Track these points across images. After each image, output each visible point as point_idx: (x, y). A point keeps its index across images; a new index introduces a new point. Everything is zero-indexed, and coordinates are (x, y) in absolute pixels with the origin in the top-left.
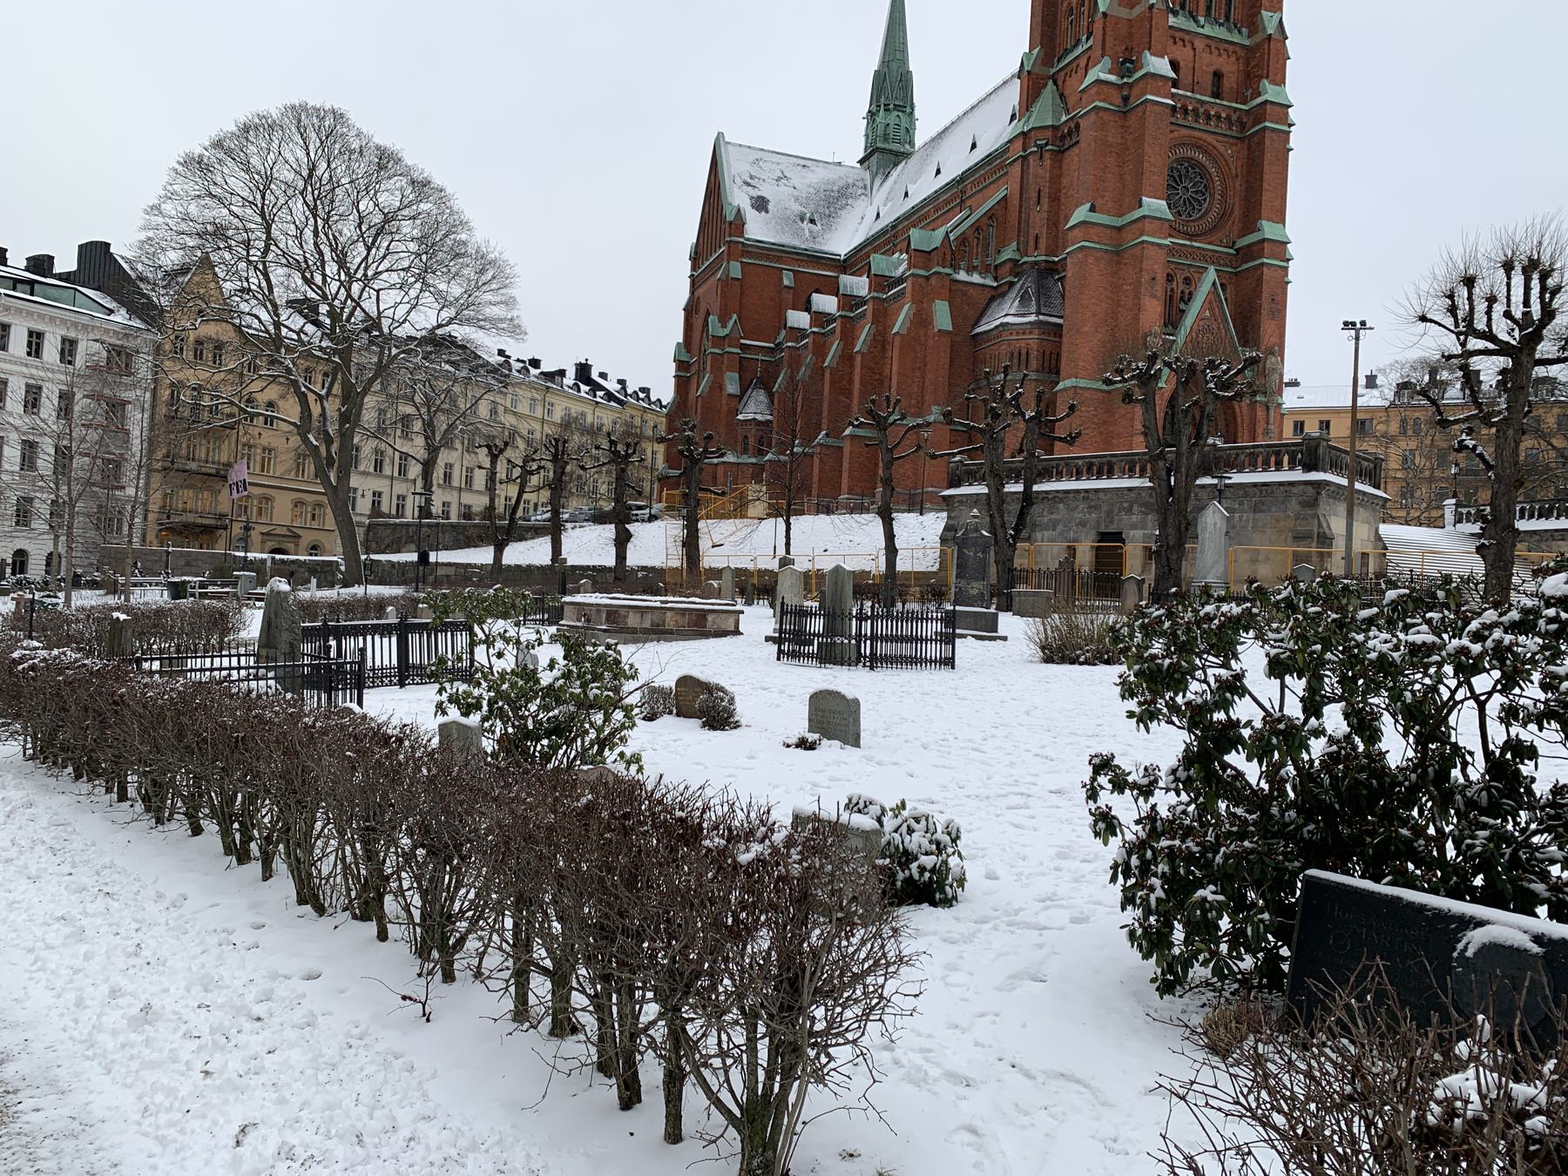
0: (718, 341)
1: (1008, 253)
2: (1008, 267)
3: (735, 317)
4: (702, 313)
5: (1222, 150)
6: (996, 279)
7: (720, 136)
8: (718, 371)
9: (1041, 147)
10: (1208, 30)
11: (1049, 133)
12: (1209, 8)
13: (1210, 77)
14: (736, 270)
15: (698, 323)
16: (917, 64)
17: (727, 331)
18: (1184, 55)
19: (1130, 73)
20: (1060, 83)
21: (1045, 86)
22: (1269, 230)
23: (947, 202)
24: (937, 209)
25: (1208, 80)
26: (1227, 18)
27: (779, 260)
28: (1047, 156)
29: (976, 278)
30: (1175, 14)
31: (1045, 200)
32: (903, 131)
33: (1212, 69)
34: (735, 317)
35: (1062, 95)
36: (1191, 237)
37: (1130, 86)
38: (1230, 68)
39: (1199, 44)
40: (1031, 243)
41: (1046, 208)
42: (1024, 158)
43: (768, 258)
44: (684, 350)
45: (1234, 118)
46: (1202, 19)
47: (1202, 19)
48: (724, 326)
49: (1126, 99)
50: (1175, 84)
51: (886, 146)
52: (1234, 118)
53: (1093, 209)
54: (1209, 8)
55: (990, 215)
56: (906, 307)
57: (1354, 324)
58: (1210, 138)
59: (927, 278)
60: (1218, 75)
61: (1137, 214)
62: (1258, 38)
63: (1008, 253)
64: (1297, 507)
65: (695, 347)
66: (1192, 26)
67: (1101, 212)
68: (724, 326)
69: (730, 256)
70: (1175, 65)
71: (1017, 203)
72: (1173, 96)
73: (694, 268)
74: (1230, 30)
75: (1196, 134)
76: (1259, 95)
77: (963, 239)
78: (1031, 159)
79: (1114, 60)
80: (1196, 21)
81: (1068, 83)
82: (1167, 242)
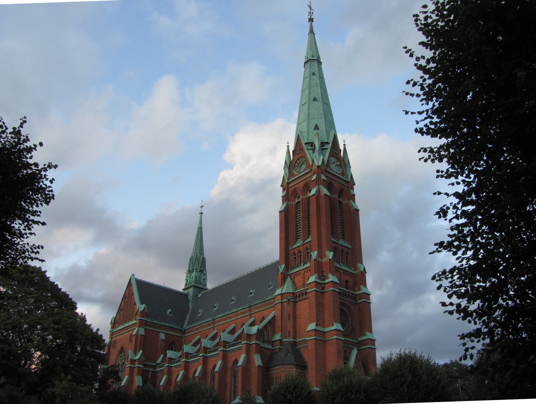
0: (133, 361)
1: (278, 337)
2: (279, 342)
6: (273, 346)
7: (133, 275)
8: (131, 374)
9: (289, 299)
10: (343, 268)
11: (292, 295)
14: (142, 332)
19: (324, 280)
20: (292, 278)
21: (287, 278)
24: (236, 315)
27: (159, 328)
31: (291, 318)
32: (202, 279)
34: (141, 351)
35: (294, 282)
37: (325, 284)
39: (341, 272)
40: (287, 334)
41: (292, 321)
42: (282, 303)
43: (154, 327)
45: (353, 296)
49: (323, 288)
52: (353, 296)
53: (317, 325)
55: (270, 322)
58: (347, 303)
60: (347, 282)
63: (278, 337)
66: (339, 266)
71: (280, 318)
72: (339, 289)
78: (285, 304)
80: (340, 265)
81: (296, 278)
82: (343, 338)
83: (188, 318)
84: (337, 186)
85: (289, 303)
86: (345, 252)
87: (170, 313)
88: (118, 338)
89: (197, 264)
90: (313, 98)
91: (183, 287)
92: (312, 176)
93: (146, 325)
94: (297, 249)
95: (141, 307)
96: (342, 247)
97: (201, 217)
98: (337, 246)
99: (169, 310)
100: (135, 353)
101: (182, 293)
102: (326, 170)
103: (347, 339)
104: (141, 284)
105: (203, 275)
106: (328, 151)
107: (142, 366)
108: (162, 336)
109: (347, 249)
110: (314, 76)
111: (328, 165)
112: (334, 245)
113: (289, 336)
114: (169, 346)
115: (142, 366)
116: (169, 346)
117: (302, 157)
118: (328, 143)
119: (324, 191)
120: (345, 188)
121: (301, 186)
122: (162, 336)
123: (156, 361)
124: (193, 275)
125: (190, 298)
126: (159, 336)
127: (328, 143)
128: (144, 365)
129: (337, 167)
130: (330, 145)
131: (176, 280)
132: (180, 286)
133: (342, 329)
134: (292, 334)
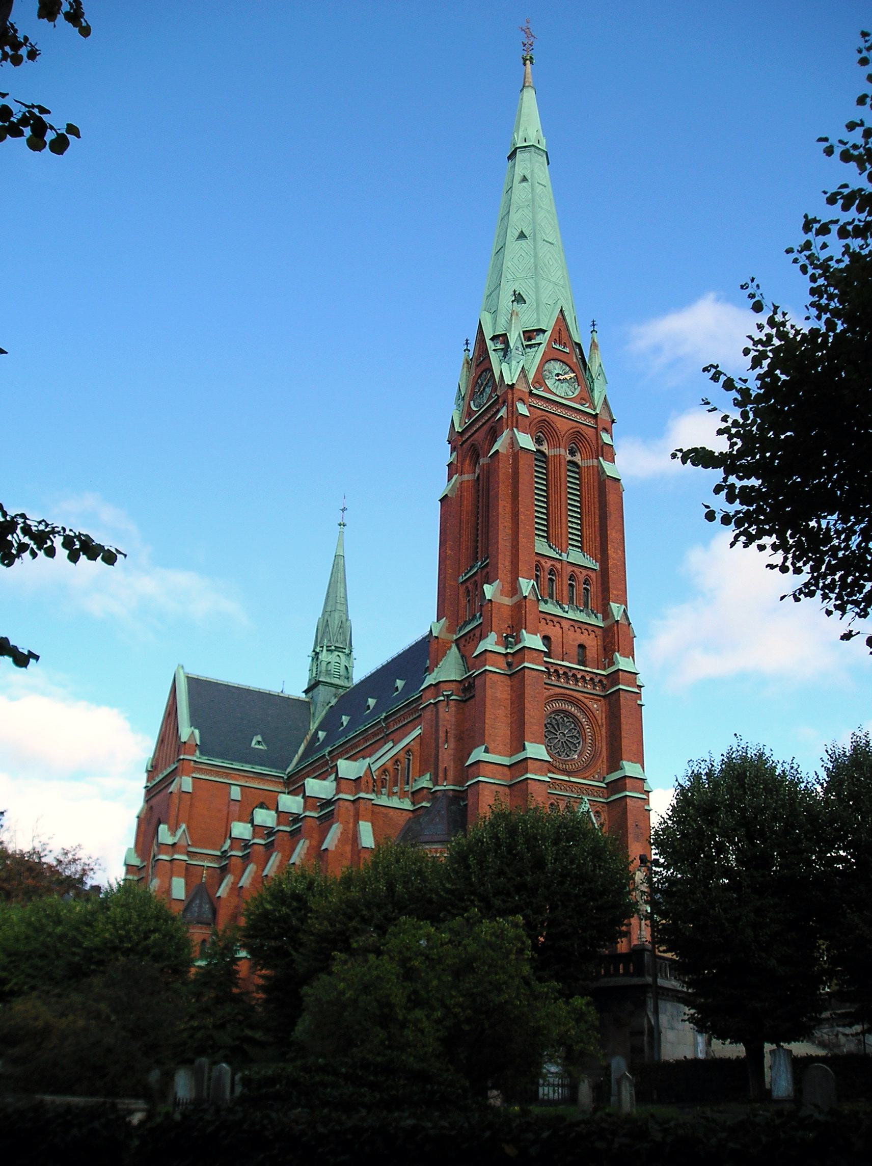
3: (184, 826)
5: (589, 704)
9: (448, 696)
10: (571, 615)
12: (571, 599)
13: (576, 649)
18: (554, 632)
22: (630, 769)
23: (374, 734)
24: (366, 740)
25: (574, 651)
26: (586, 605)
27: (227, 775)
28: (452, 703)
29: (395, 802)
30: (546, 602)
33: (577, 643)
34: (184, 826)
35: (463, 656)
36: (569, 774)
38: (592, 643)
39: (566, 624)
41: (452, 745)
43: (217, 774)
45: (597, 680)
46: (566, 607)
47: (566, 607)
50: (548, 655)
51: (328, 680)
52: (597, 680)
54: (571, 599)
61: (521, 756)
62: (609, 622)
66: (559, 612)
67: (494, 753)
68: (174, 834)
70: (546, 639)
74: (588, 615)
75: (568, 692)
76: (613, 664)
77: (384, 770)
79: (500, 635)
80: (562, 608)
84: (562, 426)
85: (448, 704)
86: (582, 578)
90: (517, 234)
91: (306, 687)
92: (498, 411)
94: (472, 581)
96: (570, 568)
98: (558, 566)
99: (259, 738)
101: (298, 701)
102: (531, 393)
103: (572, 779)
104: (195, 684)
106: (542, 348)
107: (185, 858)
108: (236, 793)
109: (585, 572)
110: (524, 184)
111: (540, 380)
112: (547, 565)
113: (445, 779)
115: (185, 858)
117: (485, 371)
118: (544, 331)
119: (526, 441)
120: (590, 432)
121: (479, 436)
122: (236, 793)
123: (222, 847)
127: (544, 331)
128: (189, 854)
129: (565, 385)
130: (548, 334)
131: (285, 674)
133: (549, 759)
134: (451, 774)
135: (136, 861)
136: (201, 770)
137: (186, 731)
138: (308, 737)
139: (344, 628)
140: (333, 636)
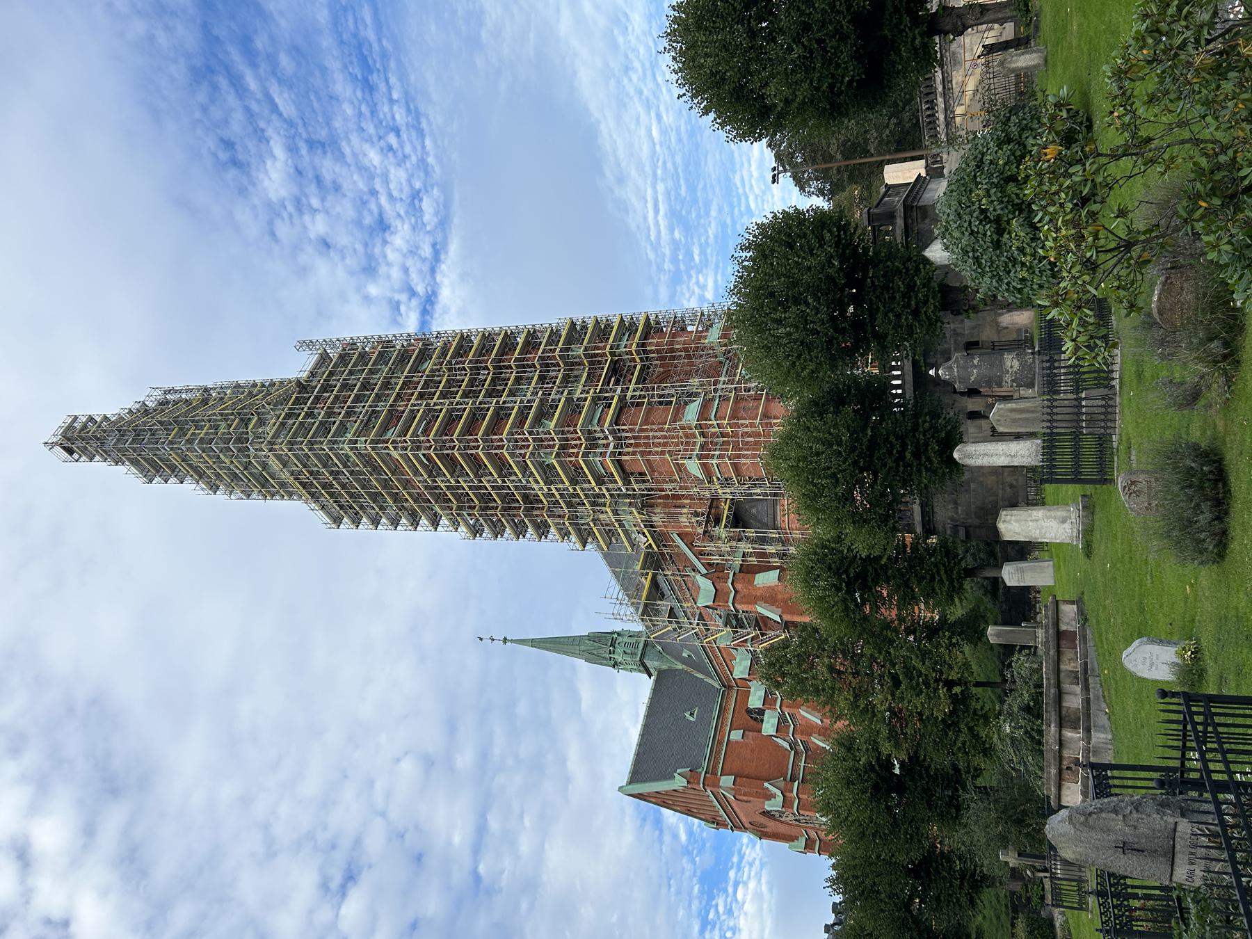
0: (787, 803)
4: (763, 820)
15: (772, 826)
16: (581, 629)
17: (779, 793)
27: (720, 743)
34: (766, 785)
43: (718, 752)
44: (796, 843)
48: (774, 796)
56: (760, 609)
57: (774, 176)
59: (736, 592)
64: (927, 221)
65: (793, 831)
68: (774, 796)
69: (716, 784)
73: (726, 826)
77: (709, 566)
83: (700, 676)
87: (692, 714)
88: (743, 819)
89: (601, 651)
91: (646, 676)
93: (714, 773)
95: (679, 782)
97: (512, 641)
100: (771, 796)
101: (656, 681)
105: (620, 639)
108: (736, 735)
114: (756, 719)
116: (756, 719)
122: (736, 735)
124: (620, 660)
125: (665, 667)
126: (737, 742)
128: (793, 779)
132: (645, 685)
135: (802, 842)
136: (715, 768)
137: (679, 782)
138: (690, 670)
139: (595, 638)
140: (601, 648)
